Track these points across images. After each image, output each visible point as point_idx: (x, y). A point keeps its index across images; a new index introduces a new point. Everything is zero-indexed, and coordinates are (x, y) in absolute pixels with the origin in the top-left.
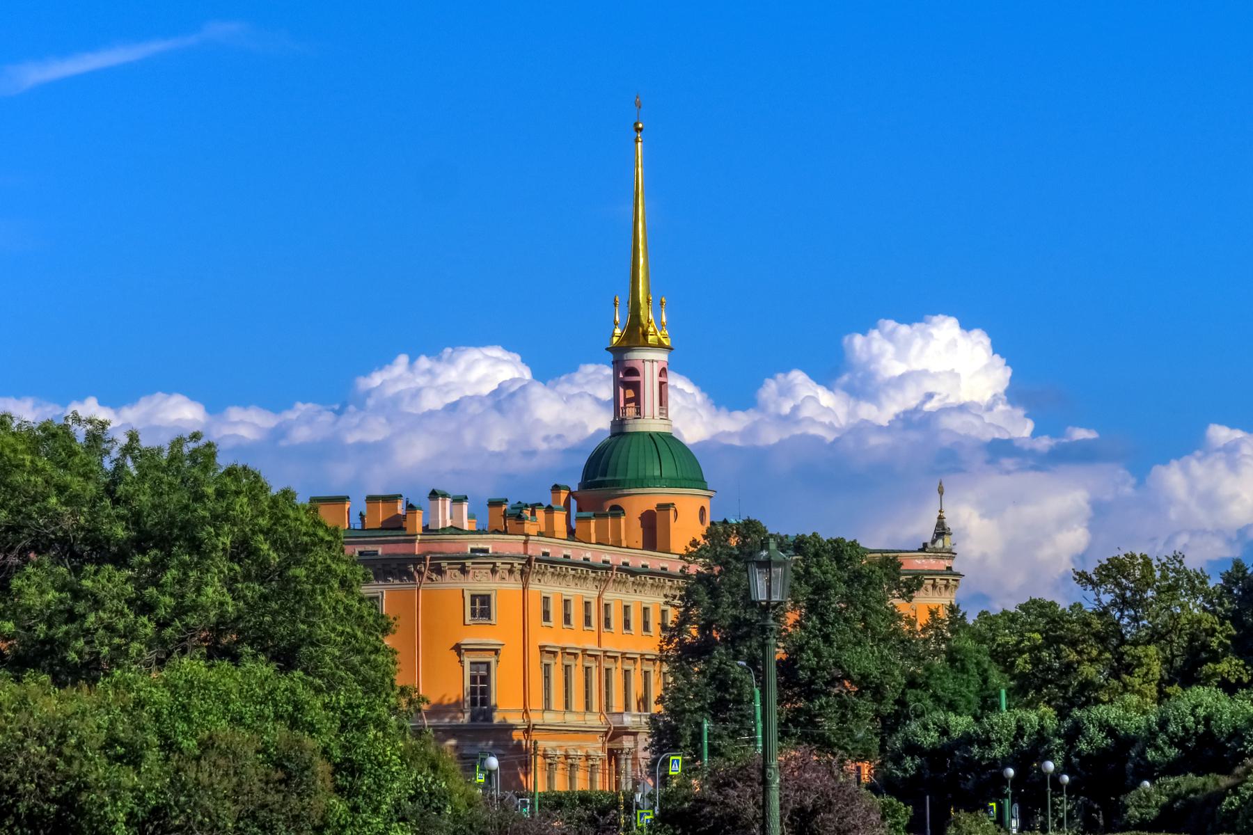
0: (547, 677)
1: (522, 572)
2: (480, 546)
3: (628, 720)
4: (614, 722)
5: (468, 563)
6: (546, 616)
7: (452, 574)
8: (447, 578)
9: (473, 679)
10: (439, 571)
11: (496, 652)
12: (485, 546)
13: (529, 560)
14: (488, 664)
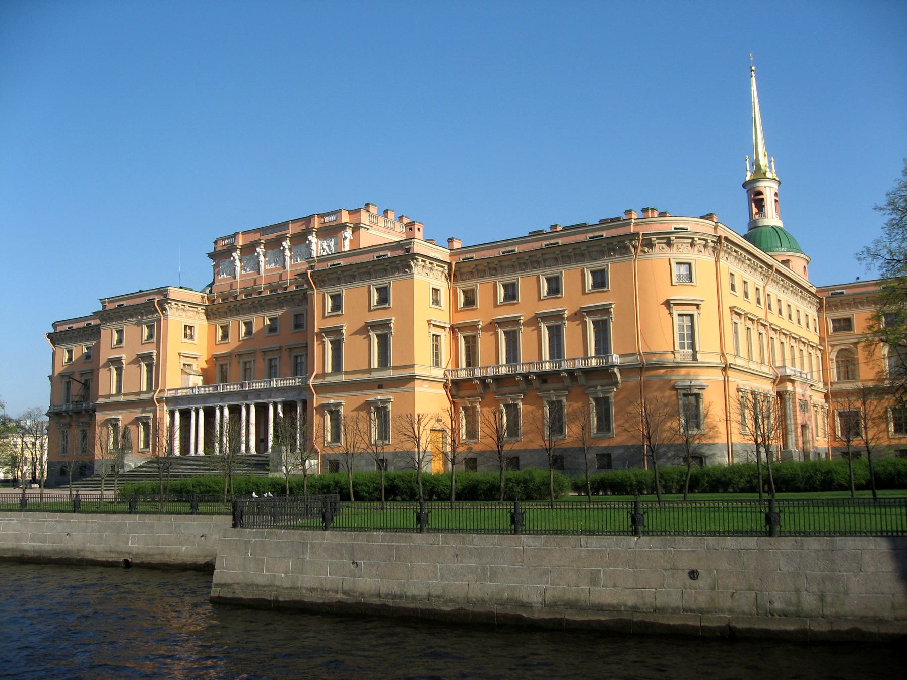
0: (736, 333)
1: (714, 248)
2: (681, 226)
3: (788, 372)
4: (780, 373)
5: (673, 237)
6: (733, 287)
7: (660, 246)
8: (656, 250)
9: (681, 327)
10: (650, 245)
11: (698, 306)
12: (685, 226)
13: (720, 237)
14: (692, 316)
